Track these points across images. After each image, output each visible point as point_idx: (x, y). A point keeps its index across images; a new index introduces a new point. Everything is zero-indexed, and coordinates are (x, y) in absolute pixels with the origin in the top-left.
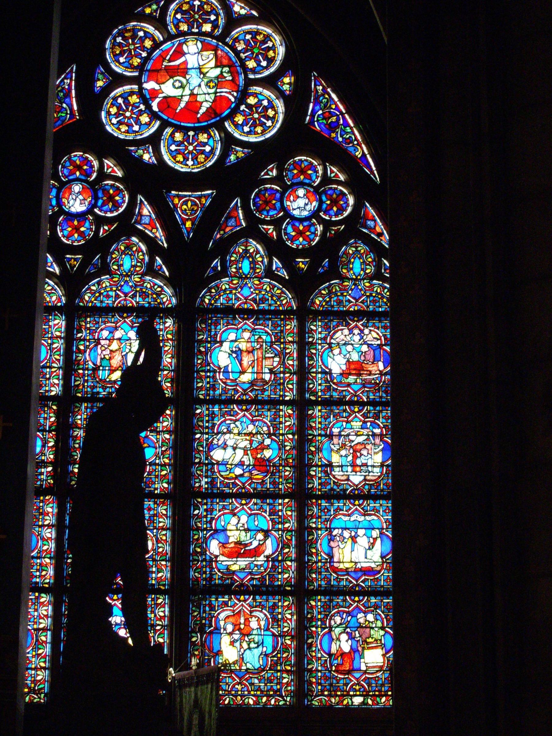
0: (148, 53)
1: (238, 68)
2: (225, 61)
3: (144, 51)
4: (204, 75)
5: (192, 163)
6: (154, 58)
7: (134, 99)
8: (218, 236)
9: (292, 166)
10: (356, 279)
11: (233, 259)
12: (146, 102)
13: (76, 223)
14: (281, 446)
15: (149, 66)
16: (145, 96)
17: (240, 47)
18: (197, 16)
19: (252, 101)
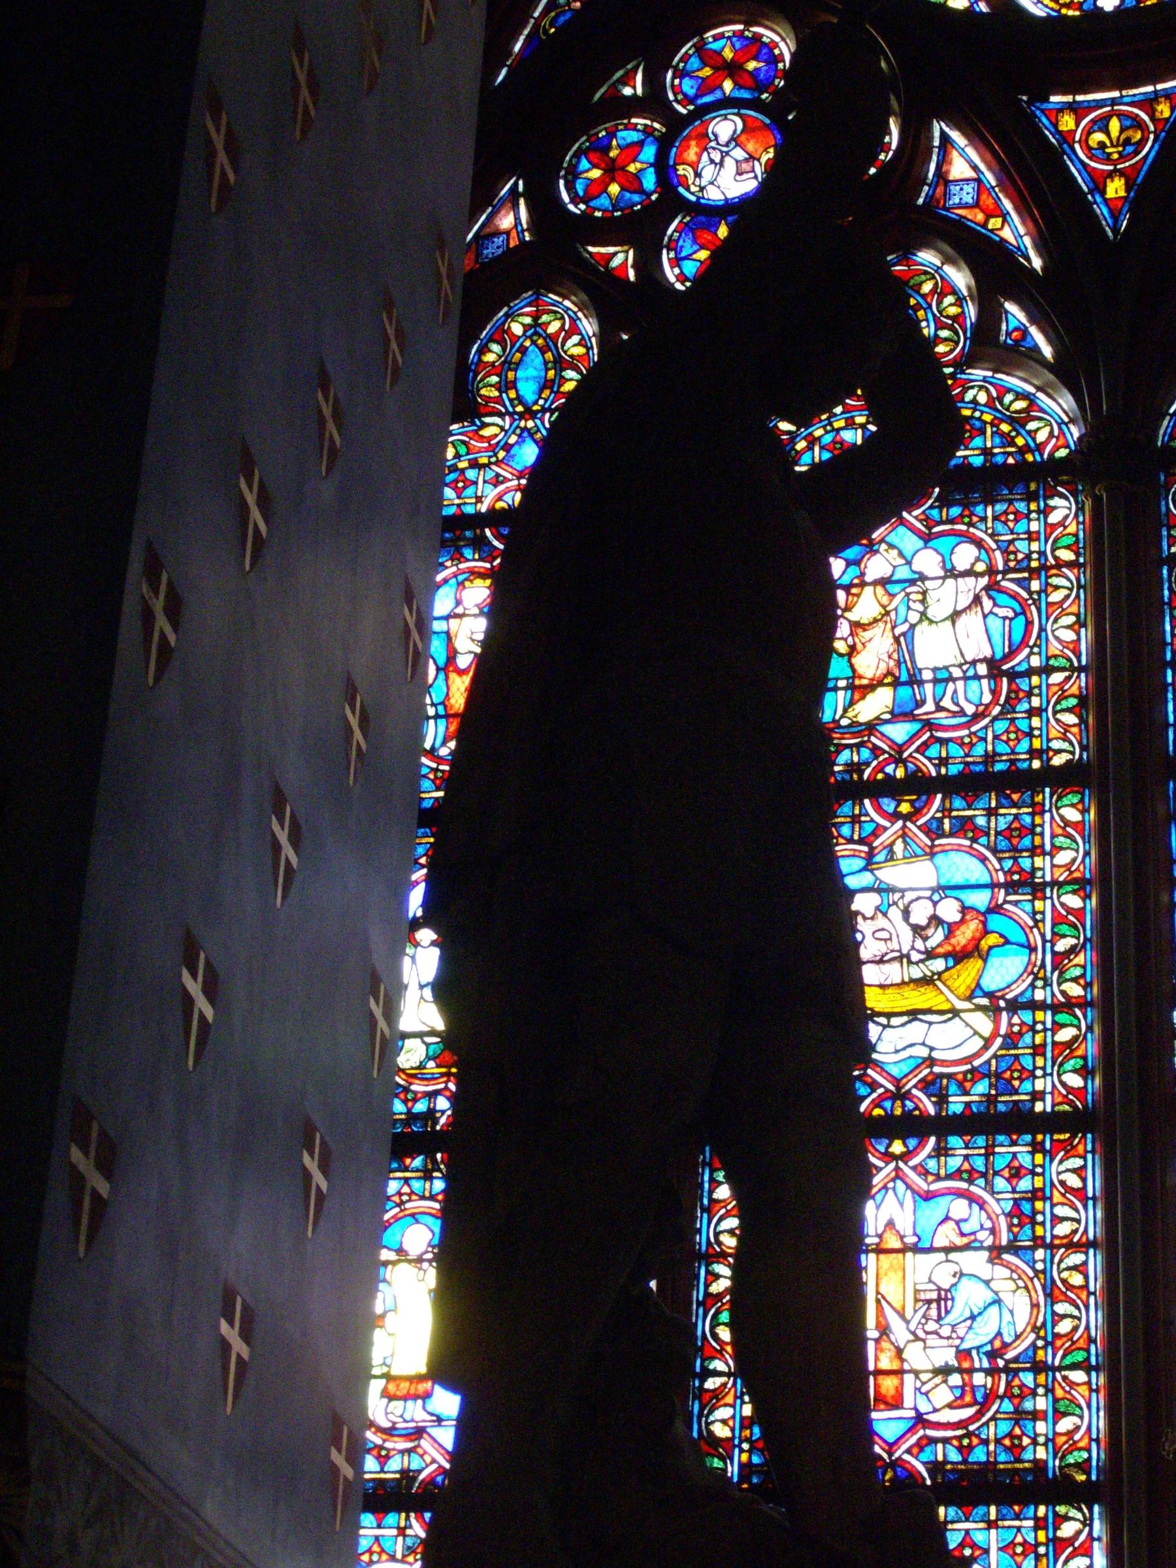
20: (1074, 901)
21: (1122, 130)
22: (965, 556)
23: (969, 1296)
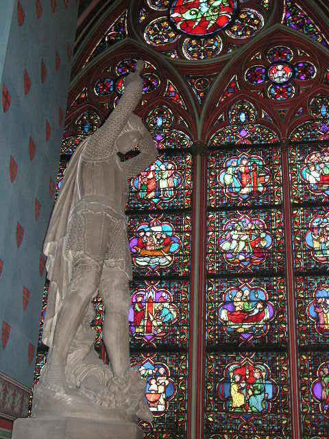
7: (165, 23)
8: (223, 100)
14: (274, 237)
19: (243, 16)
20: (187, 235)
22: (170, 166)
23: (165, 312)
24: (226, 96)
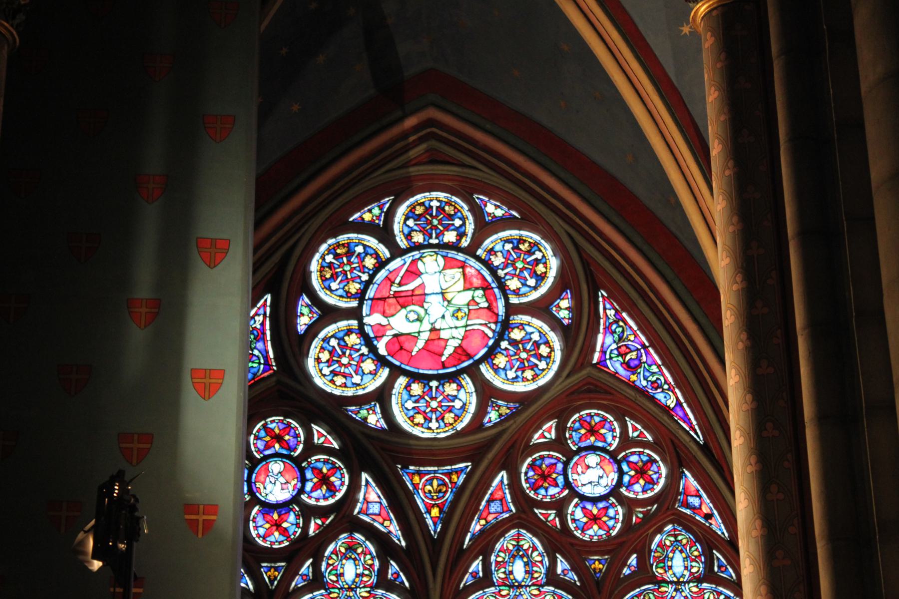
0: (370, 275)
1: (496, 290)
2: (477, 282)
3: (364, 273)
4: (449, 302)
5: (437, 425)
6: (378, 282)
7: (353, 339)
8: (478, 528)
9: (577, 425)
10: (678, 583)
11: (499, 559)
12: (368, 342)
13: (276, 516)
15: (371, 293)
16: (368, 335)
17: (497, 261)
18: (435, 222)
19: (516, 335)
21: (438, 485)
24: (485, 519)
